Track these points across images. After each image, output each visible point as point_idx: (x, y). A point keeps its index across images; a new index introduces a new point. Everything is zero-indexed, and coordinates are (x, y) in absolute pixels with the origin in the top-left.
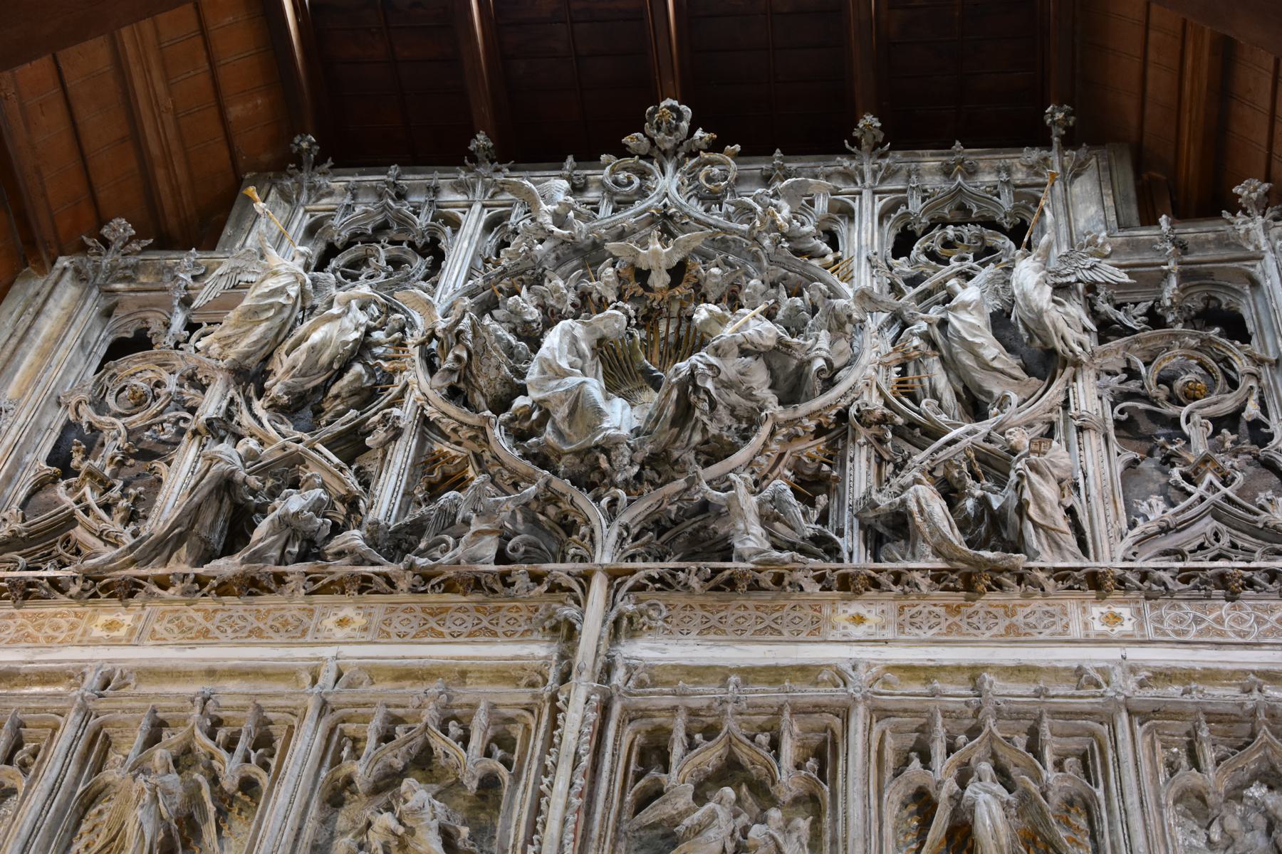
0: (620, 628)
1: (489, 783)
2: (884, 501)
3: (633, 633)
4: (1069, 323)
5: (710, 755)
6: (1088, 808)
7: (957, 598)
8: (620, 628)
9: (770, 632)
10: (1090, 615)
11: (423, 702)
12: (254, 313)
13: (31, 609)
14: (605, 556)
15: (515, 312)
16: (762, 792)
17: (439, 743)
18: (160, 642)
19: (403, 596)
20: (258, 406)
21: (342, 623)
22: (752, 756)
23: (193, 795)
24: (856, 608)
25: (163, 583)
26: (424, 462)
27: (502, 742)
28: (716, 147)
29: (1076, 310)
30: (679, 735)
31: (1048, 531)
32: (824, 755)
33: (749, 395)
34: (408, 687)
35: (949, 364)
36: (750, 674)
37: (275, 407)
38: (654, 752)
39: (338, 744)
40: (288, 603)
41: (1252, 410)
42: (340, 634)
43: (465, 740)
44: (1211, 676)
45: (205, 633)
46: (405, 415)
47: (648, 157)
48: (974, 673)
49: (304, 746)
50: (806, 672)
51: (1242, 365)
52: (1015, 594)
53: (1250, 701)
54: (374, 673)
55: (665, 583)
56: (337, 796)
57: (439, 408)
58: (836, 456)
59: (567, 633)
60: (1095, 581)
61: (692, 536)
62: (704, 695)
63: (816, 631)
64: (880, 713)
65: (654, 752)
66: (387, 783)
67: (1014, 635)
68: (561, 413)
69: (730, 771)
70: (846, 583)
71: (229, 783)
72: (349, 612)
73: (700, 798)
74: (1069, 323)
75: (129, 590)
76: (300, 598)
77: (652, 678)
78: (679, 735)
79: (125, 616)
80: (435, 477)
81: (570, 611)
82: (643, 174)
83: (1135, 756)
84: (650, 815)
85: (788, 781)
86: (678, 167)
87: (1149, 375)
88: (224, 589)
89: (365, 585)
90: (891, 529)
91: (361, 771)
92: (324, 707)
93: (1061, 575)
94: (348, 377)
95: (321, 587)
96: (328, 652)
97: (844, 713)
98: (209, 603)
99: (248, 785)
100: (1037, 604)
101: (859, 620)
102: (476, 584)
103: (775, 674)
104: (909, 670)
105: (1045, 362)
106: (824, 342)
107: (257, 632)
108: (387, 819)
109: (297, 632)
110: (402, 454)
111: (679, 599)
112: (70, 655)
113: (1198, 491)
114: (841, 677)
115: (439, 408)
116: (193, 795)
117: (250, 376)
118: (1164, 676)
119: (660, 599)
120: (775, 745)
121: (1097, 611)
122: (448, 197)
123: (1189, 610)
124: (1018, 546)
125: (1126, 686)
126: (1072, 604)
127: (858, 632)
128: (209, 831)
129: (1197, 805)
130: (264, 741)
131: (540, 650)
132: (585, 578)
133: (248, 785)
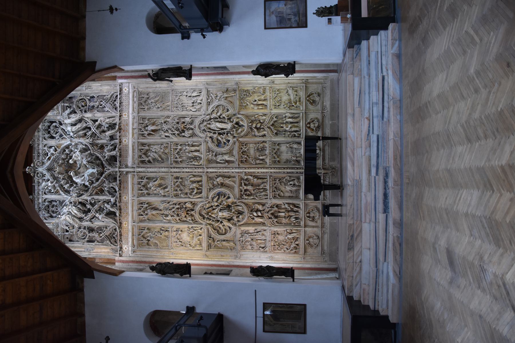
0: (127, 167)
1: (147, 178)
2: (107, 139)
3: (127, 165)
4: (74, 118)
5: (143, 156)
6: (149, 119)
7: (122, 131)
8: (127, 167)
9: (127, 151)
10: (125, 117)
11: (136, 187)
12: (73, 220)
13: (123, 234)
14: (117, 169)
15: (68, 187)
16: (147, 150)
17: (143, 184)
18: (128, 218)
19: (121, 192)
20: (85, 218)
21: (125, 198)
22: (143, 151)
23: (149, 209)
24: (123, 141)
25: (120, 220)
26: (97, 194)
27: (142, 178)
28: (34, 164)
29: (73, 115)
30: (141, 159)
31: (113, 120)
32: (143, 144)
33: (87, 155)
34: (134, 189)
35: (79, 131)
36: (133, 152)
37: (86, 216)
38: (143, 162)
39: (142, 195)
40: (123, 205)
41: (89, 98)
42: (127, 198)
43: (142, 182)
44: (133, 106)
45: (127, 213)
46: (89, 198)
47: (35, 173)
48: (133, 129)
49: (143, 199)
50: (133, 146)
51: (81, 98)
52: (122, 125)
53: (137, 103)
54: (133, 193)
55: (120, 162)
56: (149, 194)
57: (89, 194)
58: (97, 145)
59: (127, 172)
60: (120, 116)
61: (113, 160)
62: (136, 156)
63: (127, 146)
64: (138, 138)
65: (143, 162)
66: (147, 189)
67: (127, 125)
68: (91, 178)
69: (145, 154)
70: (120, 142)
71: (147, 205)
72: (124, 198)
73: (150, 156)
74: (74, 118)
75: (121, 223)
76: (122, 204)
77: (134, 163)
78: (141, 159)
79: (124, 223)
80: (101, 192)
81: (125, 173)
82: (38, 173)
83: (143, 114)
84: (152, 161)
85: (147, 148)
86: (37, 168)
87: (82, 108)
88: (120, 213)
89: (120, 196)
90: (112, 138)
91: (146, 192)
92: (138, 197)
93: (120, 119)
94: (80, 207)
95: (120, 202)
96: (130, 199)
97: (138, 142)
98: (122, 214)
99: (147, 204)
100: (123, 122)
101: (125, 141)
102: (120, 184)
103: (133, 149)
104: (133, 135)
105: (80, 121)
106: (80, 146)
107: (127, 208)
108: (152, 188)
109: (127, 203)
110: (96, 197)
111: (122, 161)
112: (130, 227)
113: (103, 104)
114: (134, 143)
115: (89, 194)
116: (149, 209)
117: (81, 219)
118: (133, 110)
119: (122, 163)
120: (142, 149)
121: (124, 116)
122: (40, 201)
123: (124, 107)
124: (115, 124)
125: (135, 114)
126: (122, 119)
127: (127, 141)
128: (153, 206)
129: (149, 109)
130: (142, 203)
131: (130, 176)
132: (120, 171)
133: (147, 204)
